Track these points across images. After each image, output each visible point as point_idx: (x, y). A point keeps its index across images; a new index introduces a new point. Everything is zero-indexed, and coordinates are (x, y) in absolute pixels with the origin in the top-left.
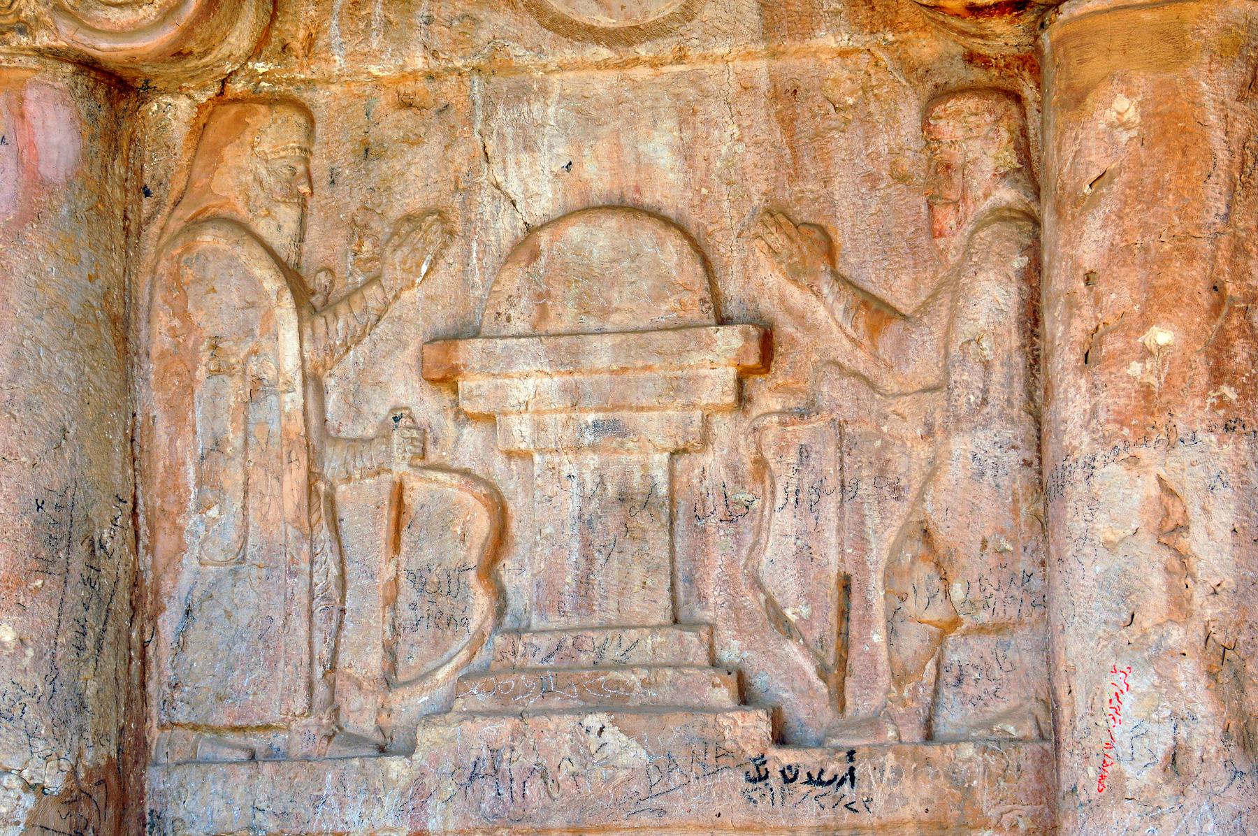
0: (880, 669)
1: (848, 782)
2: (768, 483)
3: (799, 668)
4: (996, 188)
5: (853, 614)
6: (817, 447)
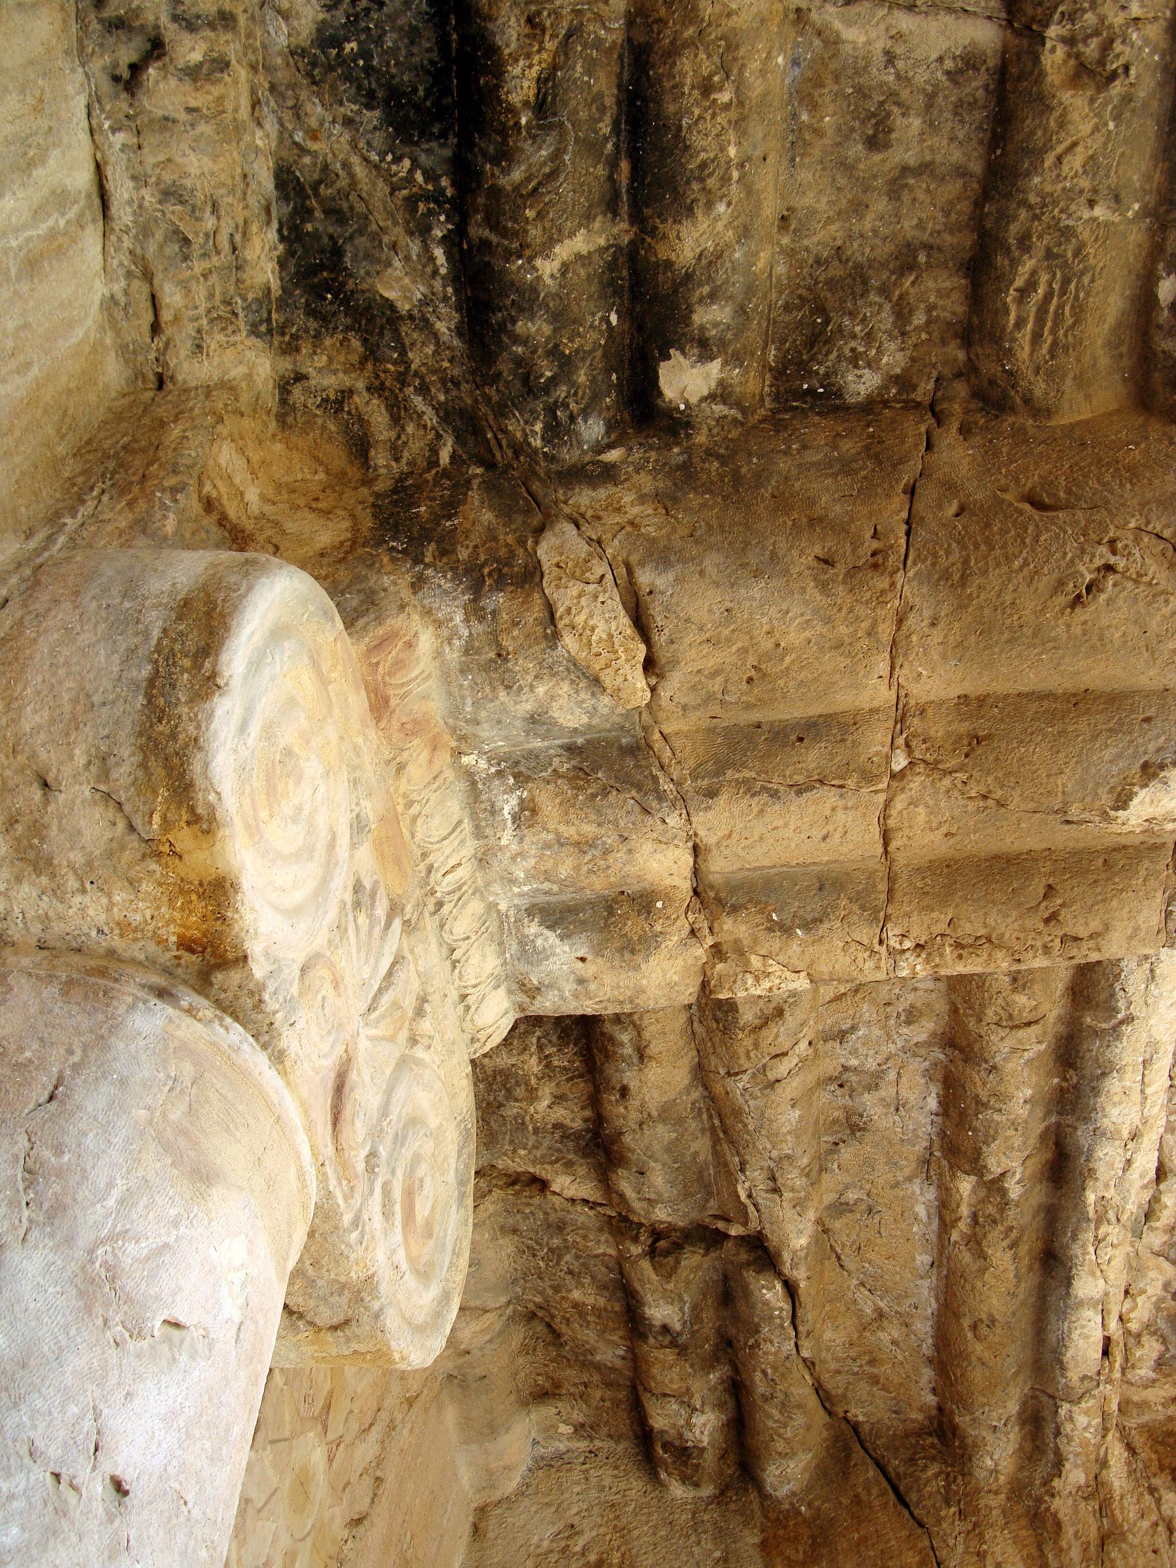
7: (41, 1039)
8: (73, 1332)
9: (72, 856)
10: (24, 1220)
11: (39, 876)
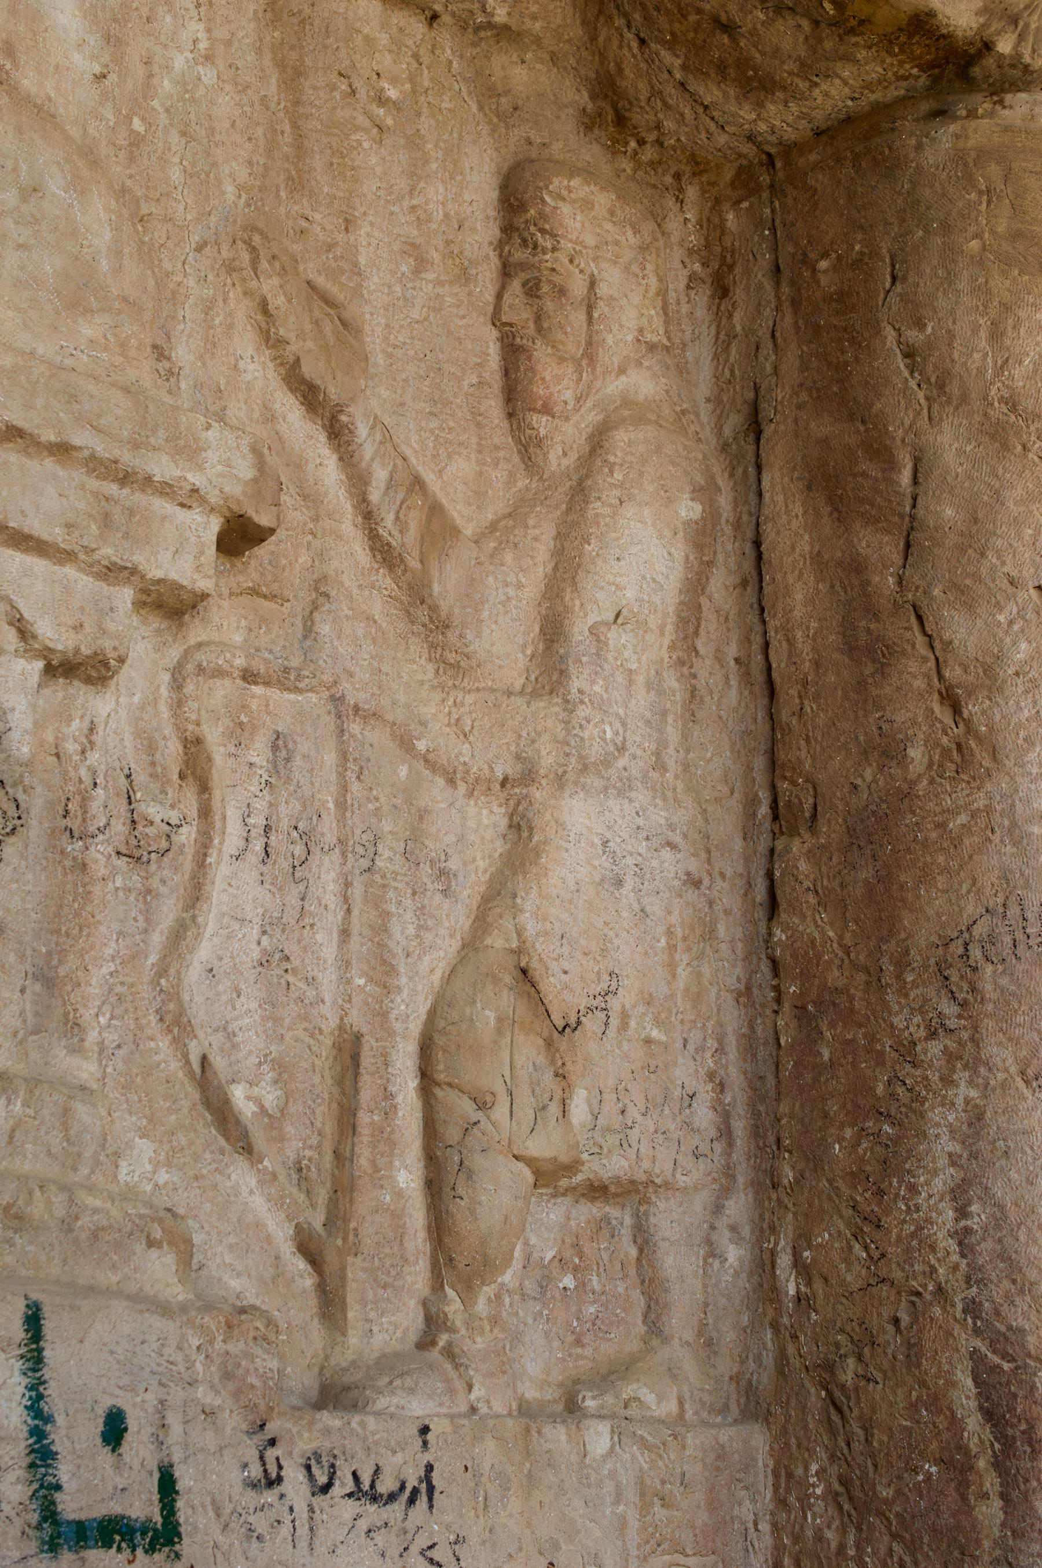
0: (410, 1246)
1: (424, 1498)
2: (217, 793)
3: (259, 1225)
4: (639, 363)
5: (364, 1118)
6: (304, 746)
7: (862, 228)
8: (1000, 471)
9: (786, 67)
10: (922, 401)
11: (773, 94)
